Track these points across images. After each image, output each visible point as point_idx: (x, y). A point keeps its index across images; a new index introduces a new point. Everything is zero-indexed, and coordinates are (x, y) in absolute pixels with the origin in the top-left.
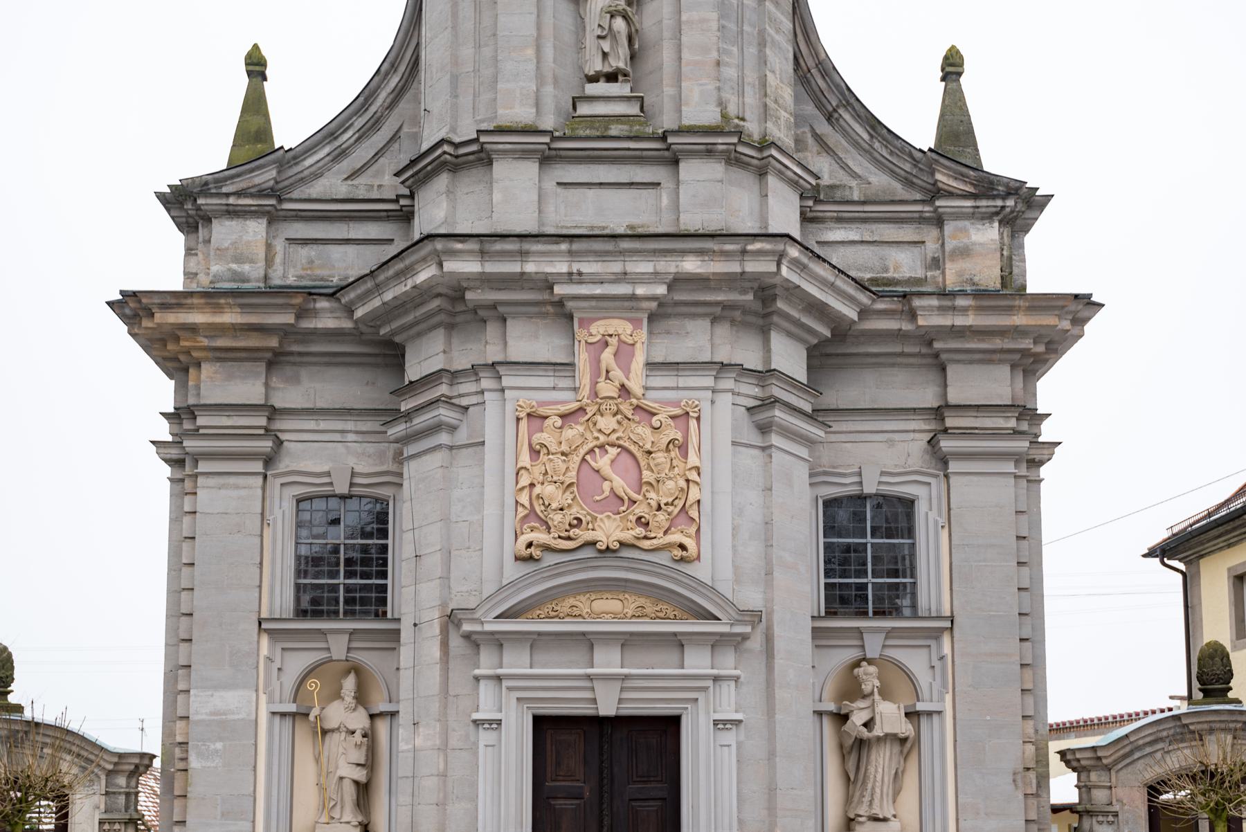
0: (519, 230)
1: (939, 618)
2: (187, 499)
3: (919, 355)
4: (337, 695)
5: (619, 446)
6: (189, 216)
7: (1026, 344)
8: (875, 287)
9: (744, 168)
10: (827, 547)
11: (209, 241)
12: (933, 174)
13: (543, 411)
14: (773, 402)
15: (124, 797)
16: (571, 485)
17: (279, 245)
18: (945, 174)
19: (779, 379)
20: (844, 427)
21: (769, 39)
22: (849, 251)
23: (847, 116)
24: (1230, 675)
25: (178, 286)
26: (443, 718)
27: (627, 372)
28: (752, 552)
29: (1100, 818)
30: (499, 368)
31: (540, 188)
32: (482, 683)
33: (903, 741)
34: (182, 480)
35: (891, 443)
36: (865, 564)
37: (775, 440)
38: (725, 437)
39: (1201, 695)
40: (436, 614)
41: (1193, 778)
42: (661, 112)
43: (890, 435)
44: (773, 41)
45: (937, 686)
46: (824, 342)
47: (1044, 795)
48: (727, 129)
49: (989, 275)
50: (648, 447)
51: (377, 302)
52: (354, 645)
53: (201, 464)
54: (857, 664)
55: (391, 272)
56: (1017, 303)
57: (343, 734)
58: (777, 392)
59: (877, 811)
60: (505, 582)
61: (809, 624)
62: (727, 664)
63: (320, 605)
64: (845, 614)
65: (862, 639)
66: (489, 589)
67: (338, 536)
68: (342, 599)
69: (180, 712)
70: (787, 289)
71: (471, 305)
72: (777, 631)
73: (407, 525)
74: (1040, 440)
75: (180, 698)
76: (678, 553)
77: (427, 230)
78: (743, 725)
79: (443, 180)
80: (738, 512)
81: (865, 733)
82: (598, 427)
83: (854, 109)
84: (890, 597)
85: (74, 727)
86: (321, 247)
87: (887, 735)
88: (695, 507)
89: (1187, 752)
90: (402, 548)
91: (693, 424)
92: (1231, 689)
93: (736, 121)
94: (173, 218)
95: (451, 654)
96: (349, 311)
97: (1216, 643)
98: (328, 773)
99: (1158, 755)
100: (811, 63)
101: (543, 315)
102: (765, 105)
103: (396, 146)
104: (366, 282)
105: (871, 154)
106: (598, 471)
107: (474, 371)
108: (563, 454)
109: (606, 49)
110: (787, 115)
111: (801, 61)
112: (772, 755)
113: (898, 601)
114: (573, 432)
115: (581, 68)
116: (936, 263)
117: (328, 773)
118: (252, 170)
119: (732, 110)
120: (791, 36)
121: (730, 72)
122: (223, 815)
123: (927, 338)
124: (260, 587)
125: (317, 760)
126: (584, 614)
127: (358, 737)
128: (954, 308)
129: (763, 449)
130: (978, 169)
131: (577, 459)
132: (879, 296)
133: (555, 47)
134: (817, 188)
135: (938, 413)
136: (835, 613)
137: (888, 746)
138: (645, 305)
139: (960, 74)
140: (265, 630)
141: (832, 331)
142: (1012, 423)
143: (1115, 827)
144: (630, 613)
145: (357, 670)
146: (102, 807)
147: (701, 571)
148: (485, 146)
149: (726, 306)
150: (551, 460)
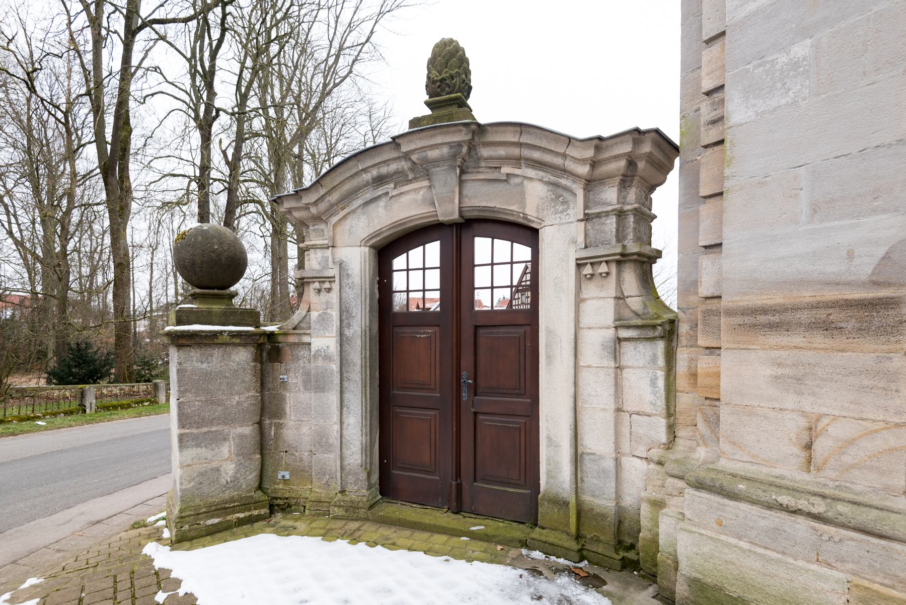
15: (614, 220)
122: (815, 209)
146: (581, 239)
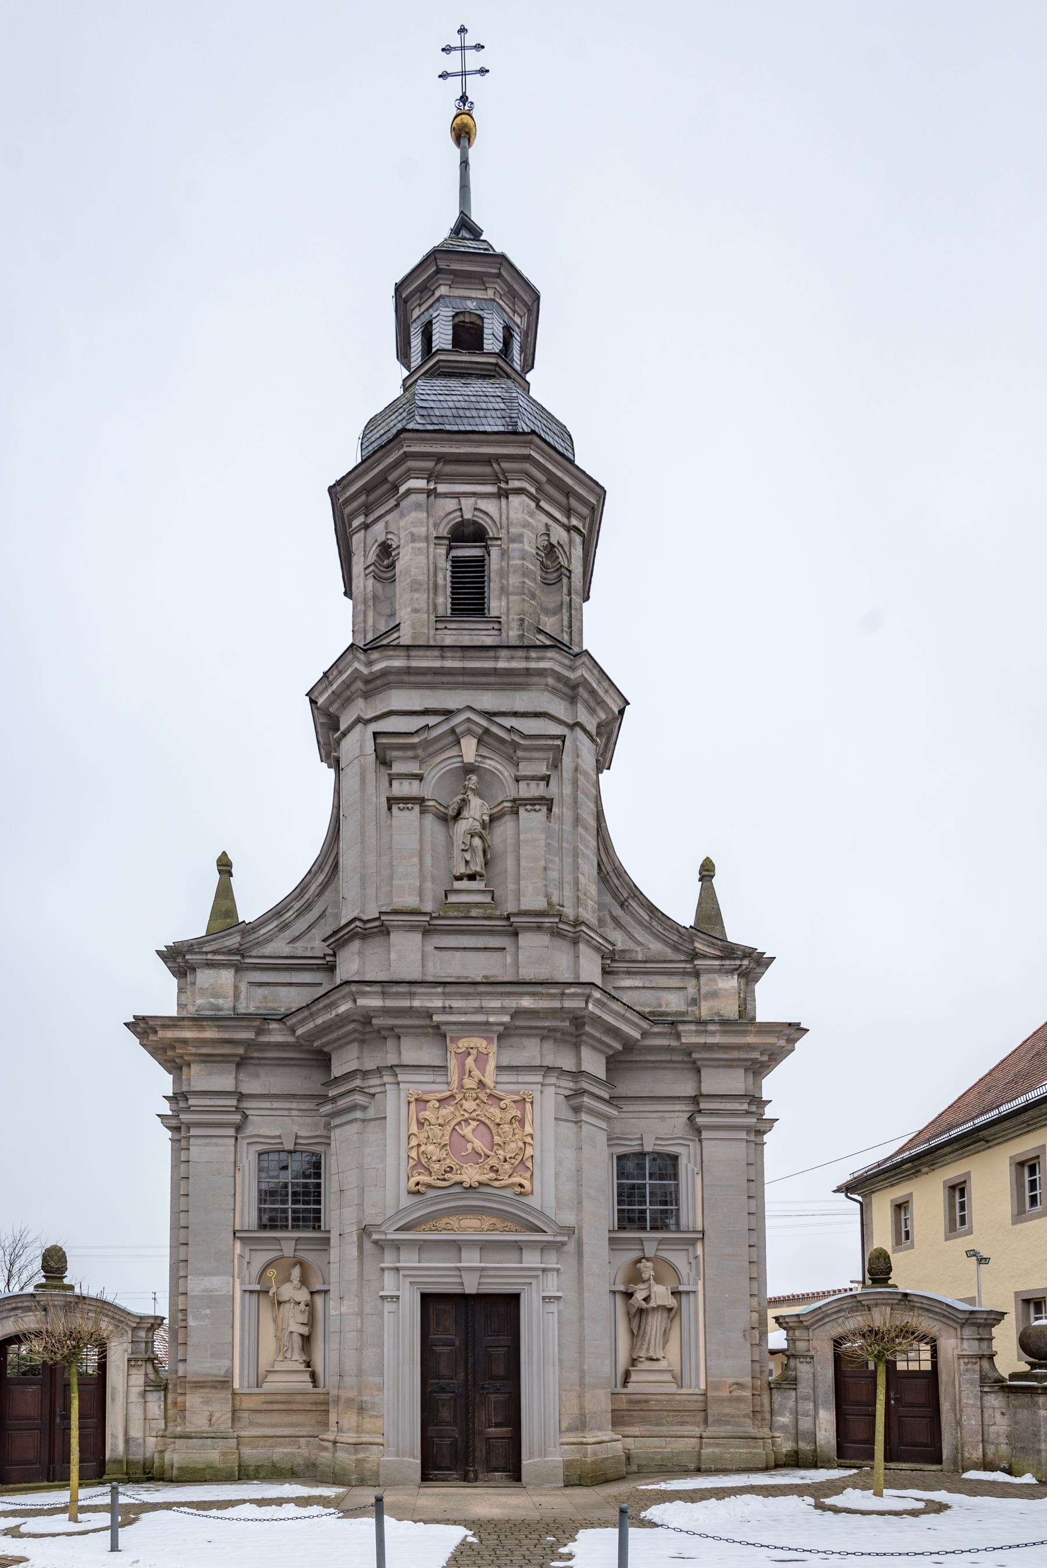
0: (408, 978)
1: (695, 1232)
2: (183, 1152)
3: (683, 1062)
4: (288, 1279)
5: (478, 1120)
6: (180, 967)
7: (755, 1055)
8: (653, 1017)
9: (563, 939)
10: (619, 1185)
11: (195, 984)
12: (693, 943)
13: (426, 1097)
14: (581, 1092)
16: (446, 1145)
17: (243, 987)
18: (700, 943)
19: (587, 1077)
20: (631, 1108)
21: (580, 853)
22: (635, 994)
23: (634, 904)
24: (890, 1269)
25: (174, 1014)
26: (360, 1295)
27: (483, 1073)
28: (568, 1188)
29: (802, 1360)
30: (396, 1069)
31: (423, 951)
32: (386, 1272)
33: (670, 1310)
34: (180, 1140)
35: (663, 1119)
36: (645, 1197)
37: (584, 1117)
38: (550, 1115)
39: (870, 1282)
40: (354, 1228)
41: (864, 1336)
42: (506, 901)
43: (662, 1114)
44: (583, 854)
45: (693, 1275)
46: (618, 1053)
47: (765, 1345)
48: (551, 913)
49: (731, 1010)
50: (498, 1121)
51: (311, 1025)
52: (299, 1247)
53: (192, 1130)
54: (639, 1261)
55: (321, 1005)
56: (749, 1028)
57: (292, 1304)
58: (585, 1085)
59: (652, 1354)
60: (401, 1208)
61: (607, 1235)
62: (552, 1261)
63: (275, 1221)
64: (632, 1228)
65: (642, 1245)
66: (390, 1212)
67: (287, 1177)
68: (290, 1218)
69: (181, 1290)
70: (592, 1019)
71: (376, 1028)
72: (585, 1239)
73: (334, 1170)
74: (764, 1117)
75: (181, 1281)
76: (518, 1189)
77: (346, 978)
78: (562, 1300)
79: (356, 945)
80: (559, 1163)
81: (644, 1305)
82: (463, 1108)
83: (639, 899)
84: (662, 1219)
85: (109, 1298)
86: (272, 988)
87: (659, 1306)
88: (530, 1160)
89: (859, 1318)
90: (331, 1184)
91: (528, 1106)
92: (890, 1278)
93: (558, 907)
94: (169, 968)
95: (365, 1253)
96: (292, 1030)
97: (881, 1249)
98: (283, 1329)
99: (840, 1321)
100: (609, 869)
101: (426, 1035)
102: (578, 897)
103: (323, 921)
104: (303, 1012)
105: (650, 930)
106: (464, 1137)
107: (379, 1071)
108: (440, 1125)
109: (468, 859)
110: (592, 903)
111: (603, 867)
112: (581, 1318)
113: (667, 1221)
114: (447, 1111)
115: (451, 871)
116: (695, 1002)
117: (283, 1329)
118: (224, 937)
119: (555, 899)
120: (596, 851)
121: (554, 875)
122: (211, 1355)
123: (688, 1051)
124: (234, 1210)
125: (275, 1321)
126: (455, 1228)
127: (302, 1306)
128: (706, 1032)
129: (576, 1122)
130: (724, 940)
131: (449, 1128)
132: (655, 1023)
133: (432, 857)
134: (613, 952)
135: (695, 1099)
136: (624, 1228)
137: (660, 1313)
138: (495, 1028)
139: (712, 877)
140: (238, 1238)
141: (624, 1046)
142: (745, 1107)
143: (811, 1365)
144: (486, 1228)
145: (301, 1263)
146: (130, 1350)
147: (534, 1201)
148: (385, 922)
149: (551, 1030)
150: (432, 1129)
